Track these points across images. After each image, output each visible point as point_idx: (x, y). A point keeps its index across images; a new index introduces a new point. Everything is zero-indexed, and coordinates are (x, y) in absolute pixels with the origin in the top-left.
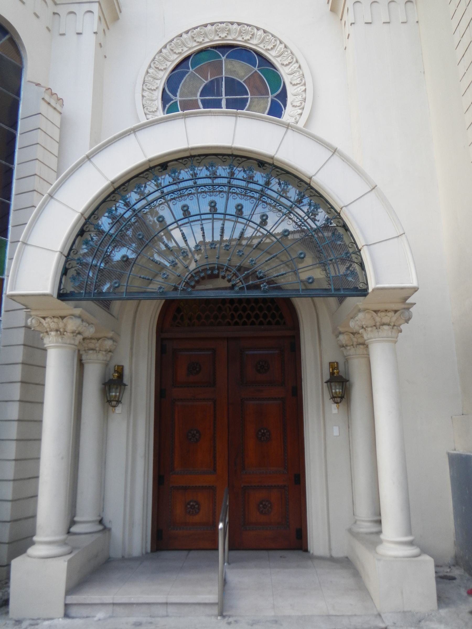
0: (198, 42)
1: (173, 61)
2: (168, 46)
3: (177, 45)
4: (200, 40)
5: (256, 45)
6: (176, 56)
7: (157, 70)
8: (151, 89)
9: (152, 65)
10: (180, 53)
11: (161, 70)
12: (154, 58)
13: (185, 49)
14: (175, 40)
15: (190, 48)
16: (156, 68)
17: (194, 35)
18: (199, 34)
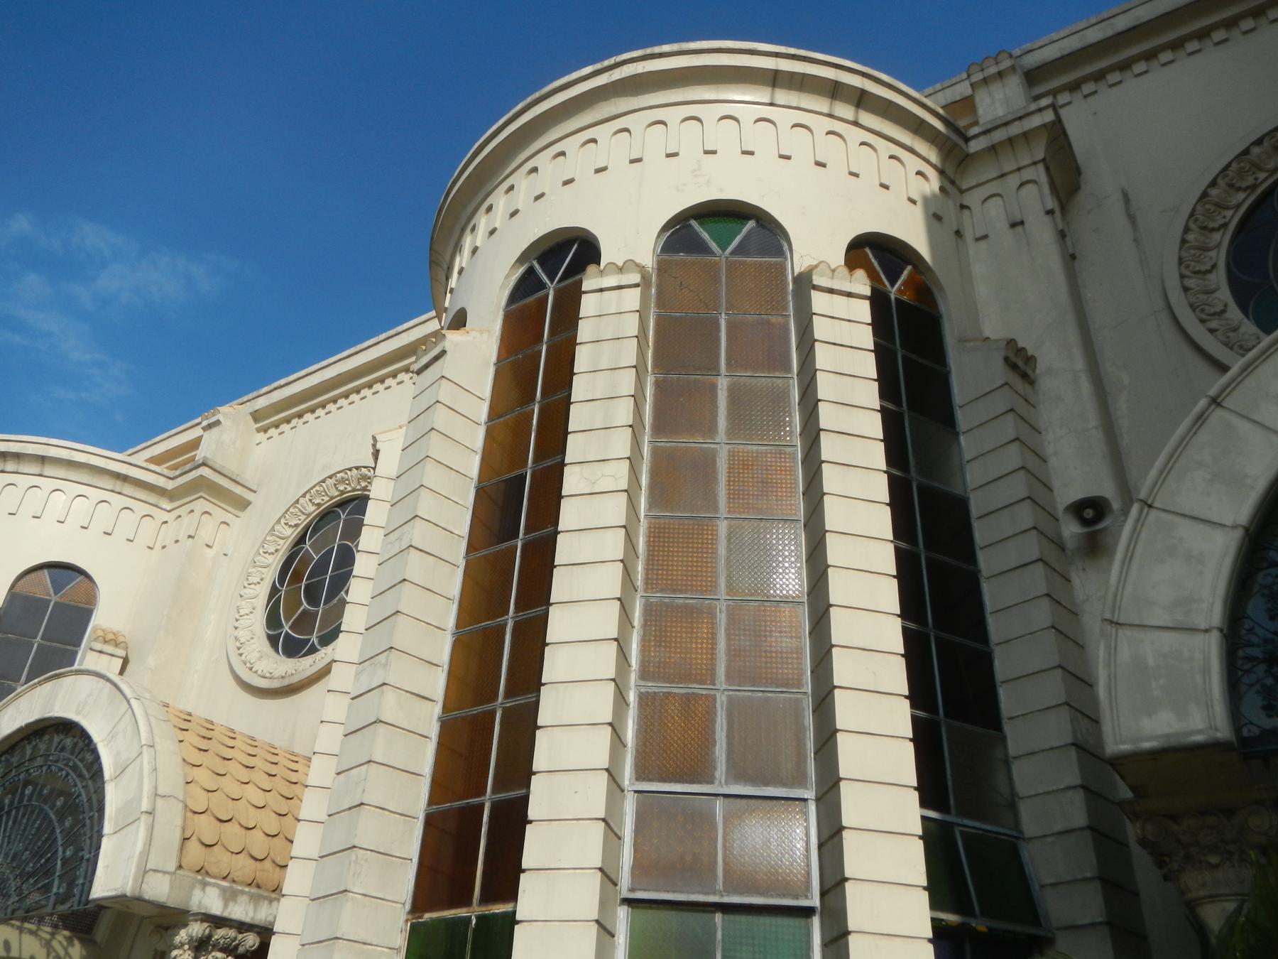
0: (340, 491)
1: (309, 515)
2: (308, 496)
4: (341, 488)
6: (311, 508)
7: (286, 527)
9: (283, 521)
10: (319, 505)
11: (290, 526)
12: (288, 510)
13: (326, 499)
14: (317, 488)
15: (332, 498)
16: (286, 524)
17: (336, 481)
18: (343, 481)
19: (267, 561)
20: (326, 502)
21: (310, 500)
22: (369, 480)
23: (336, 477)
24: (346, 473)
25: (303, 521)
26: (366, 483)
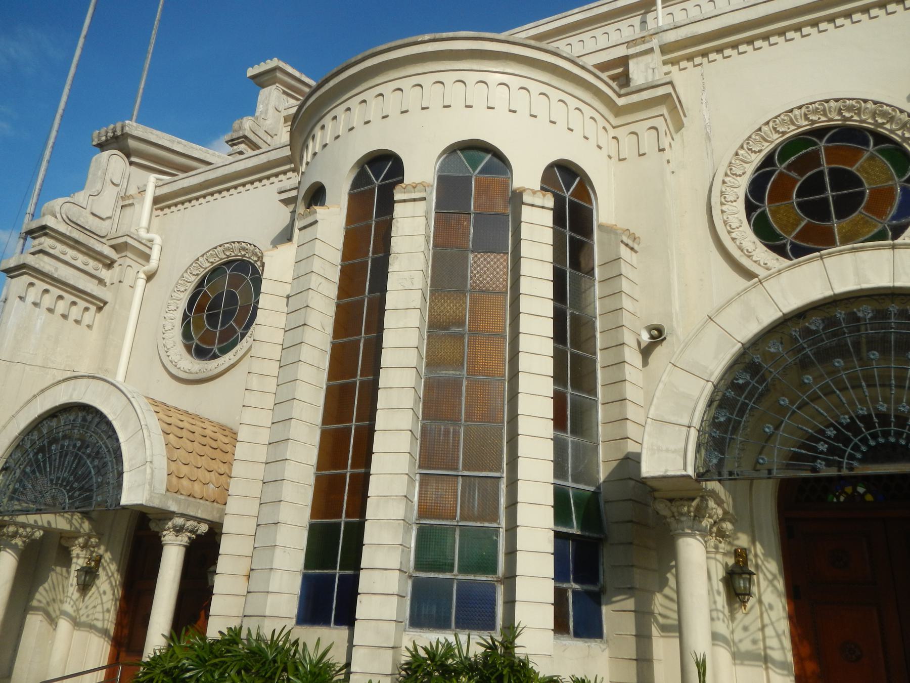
0: (812, 120)
1: (772, 142)
2: (771, 124)
3: (783, 122)
5: (892, 131)
8: (735, 174)
10: (784, 133)
12: (750, 137)
14: (782, 116)
17: (809, 111)
18: (816, 111)
19: (736, 182)
20: (792, 131)
21: (775, 129)
22: (856, 111)
23: (808, 107)
24: (820, 104)
25: (767, 148)
26: (853, 114)
